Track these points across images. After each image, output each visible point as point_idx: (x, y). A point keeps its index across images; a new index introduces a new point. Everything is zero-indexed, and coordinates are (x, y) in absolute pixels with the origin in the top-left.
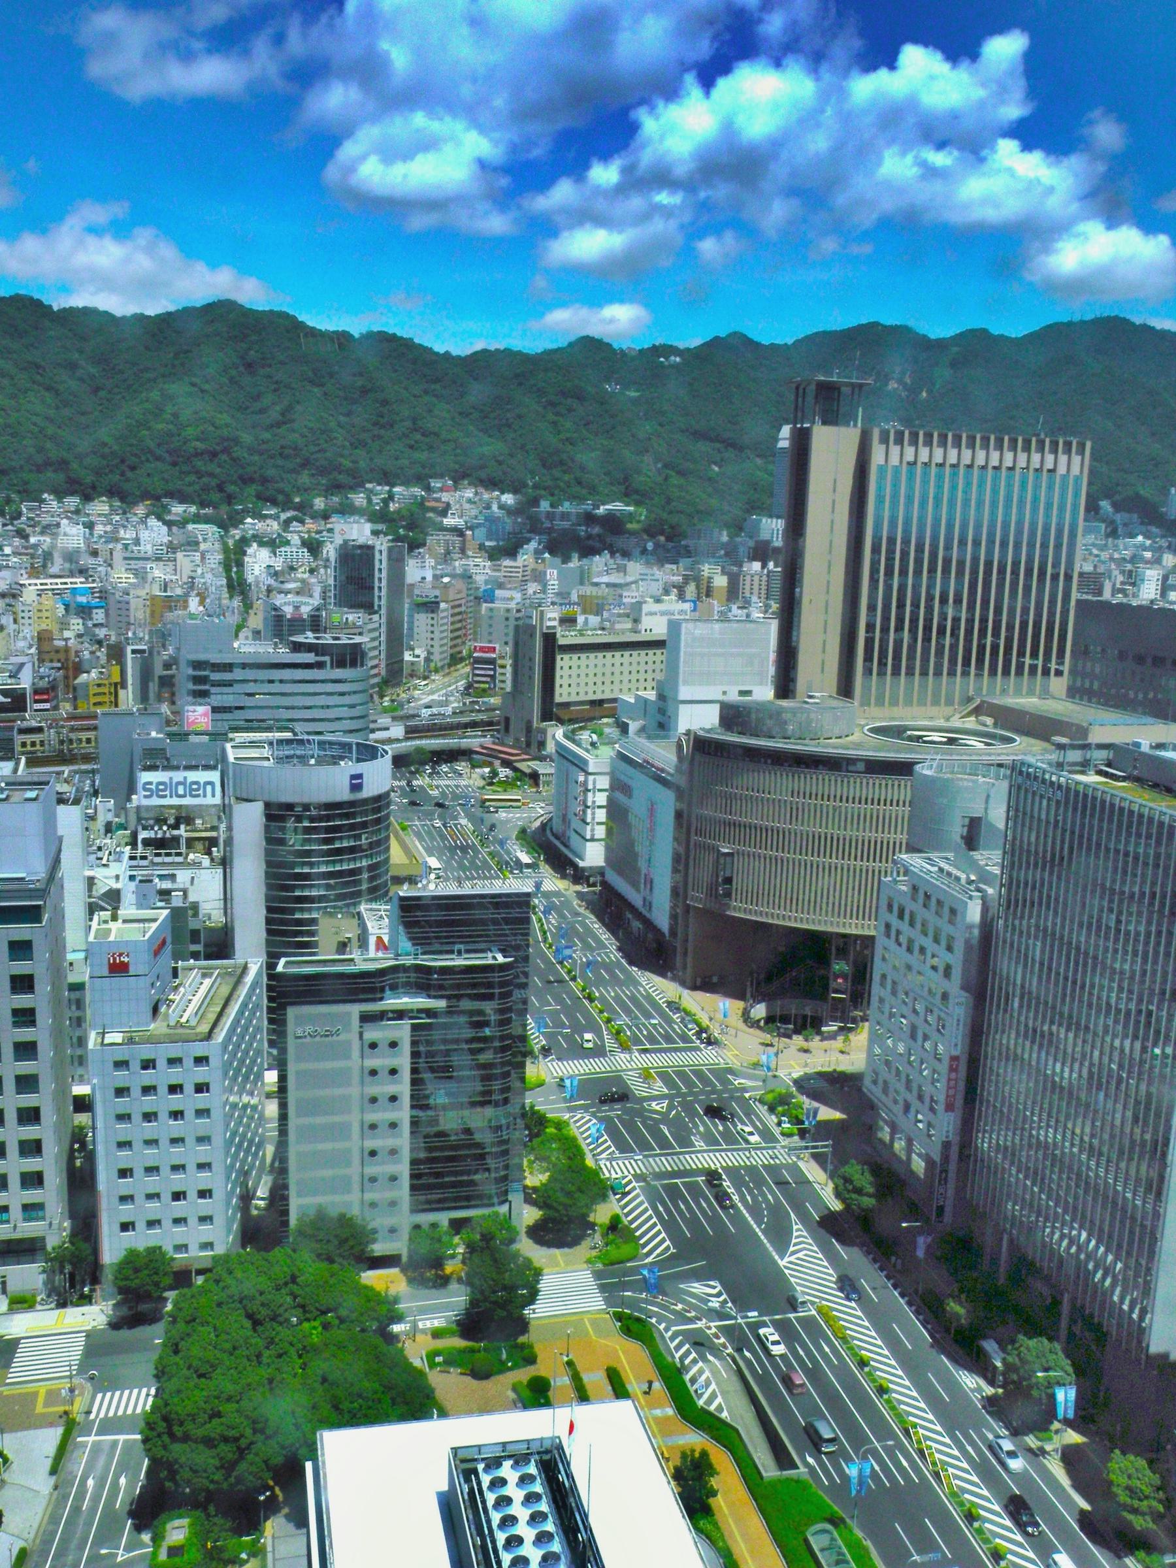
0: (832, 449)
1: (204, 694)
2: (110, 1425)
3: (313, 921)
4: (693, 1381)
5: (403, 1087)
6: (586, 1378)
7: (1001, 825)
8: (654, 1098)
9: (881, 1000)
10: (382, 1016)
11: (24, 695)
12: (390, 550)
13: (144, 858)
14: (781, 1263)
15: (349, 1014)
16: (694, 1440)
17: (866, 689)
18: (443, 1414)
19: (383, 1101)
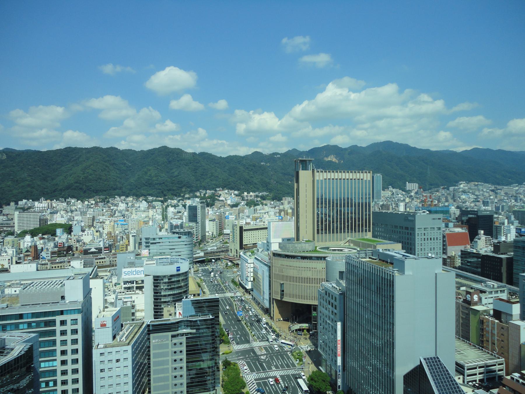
0: (305, 176)
1: (149, 246)
5: (184, 356)
10: (178, 335)
12: (201, 206)
15: (168, 335)
19: (178, 361)
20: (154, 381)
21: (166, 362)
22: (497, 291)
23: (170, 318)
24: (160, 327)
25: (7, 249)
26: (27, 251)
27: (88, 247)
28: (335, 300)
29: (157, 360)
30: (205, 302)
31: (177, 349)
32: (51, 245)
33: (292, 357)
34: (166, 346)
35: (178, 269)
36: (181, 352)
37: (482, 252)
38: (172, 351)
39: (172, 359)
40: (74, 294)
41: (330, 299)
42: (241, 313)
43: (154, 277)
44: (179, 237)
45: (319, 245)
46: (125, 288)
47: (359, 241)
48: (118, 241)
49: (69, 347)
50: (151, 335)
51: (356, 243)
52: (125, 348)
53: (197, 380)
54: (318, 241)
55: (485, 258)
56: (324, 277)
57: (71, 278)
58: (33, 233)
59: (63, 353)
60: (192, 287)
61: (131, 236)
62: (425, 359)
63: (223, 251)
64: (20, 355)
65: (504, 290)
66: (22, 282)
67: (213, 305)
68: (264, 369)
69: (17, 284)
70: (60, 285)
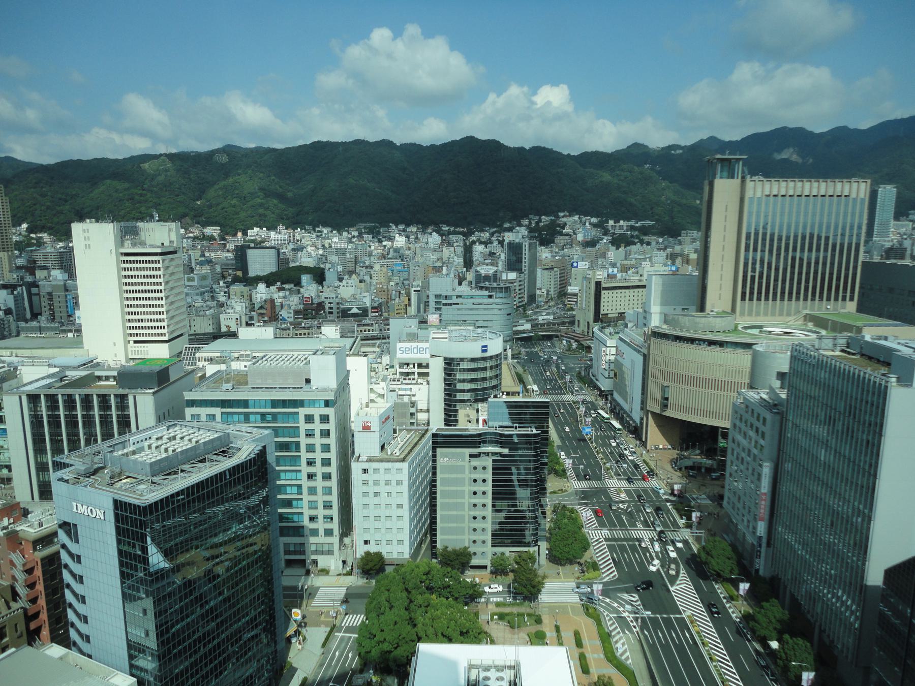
0: (725, 189)
2: (349, 630)
4: (617, 642)
5: (489, 488)
6: (554, 634)
8: (622, 502)
10: (478, 455)
12: (530, 245)
16: (610, 671)
17: (743, 308)
18: (493, 642)
23: (469, 426)
25: (234, 304)
26: (261, 308)
27: (347, 305)
29: (447, 488)
31: (479, 476)
32: (295, 299)
34: (461, 469)
35: (484, 349)
39: (470, 491)
40: (324, 376)
42: (589, 430)
44: (490, 297)
46: (402, 374)
48: (393, 297)
49: (318, 456)
51: (820, 322)
53: (508, 527)
54: (742, 314)
56: (747, 381)
58: (269, 280)
59: (310, 463)
60: (508, 381)
61: (412, 290)
63: (563, 324)
66: (254, 354)
67: (540, 412)
68: (622, 524)
69: (247, 356)
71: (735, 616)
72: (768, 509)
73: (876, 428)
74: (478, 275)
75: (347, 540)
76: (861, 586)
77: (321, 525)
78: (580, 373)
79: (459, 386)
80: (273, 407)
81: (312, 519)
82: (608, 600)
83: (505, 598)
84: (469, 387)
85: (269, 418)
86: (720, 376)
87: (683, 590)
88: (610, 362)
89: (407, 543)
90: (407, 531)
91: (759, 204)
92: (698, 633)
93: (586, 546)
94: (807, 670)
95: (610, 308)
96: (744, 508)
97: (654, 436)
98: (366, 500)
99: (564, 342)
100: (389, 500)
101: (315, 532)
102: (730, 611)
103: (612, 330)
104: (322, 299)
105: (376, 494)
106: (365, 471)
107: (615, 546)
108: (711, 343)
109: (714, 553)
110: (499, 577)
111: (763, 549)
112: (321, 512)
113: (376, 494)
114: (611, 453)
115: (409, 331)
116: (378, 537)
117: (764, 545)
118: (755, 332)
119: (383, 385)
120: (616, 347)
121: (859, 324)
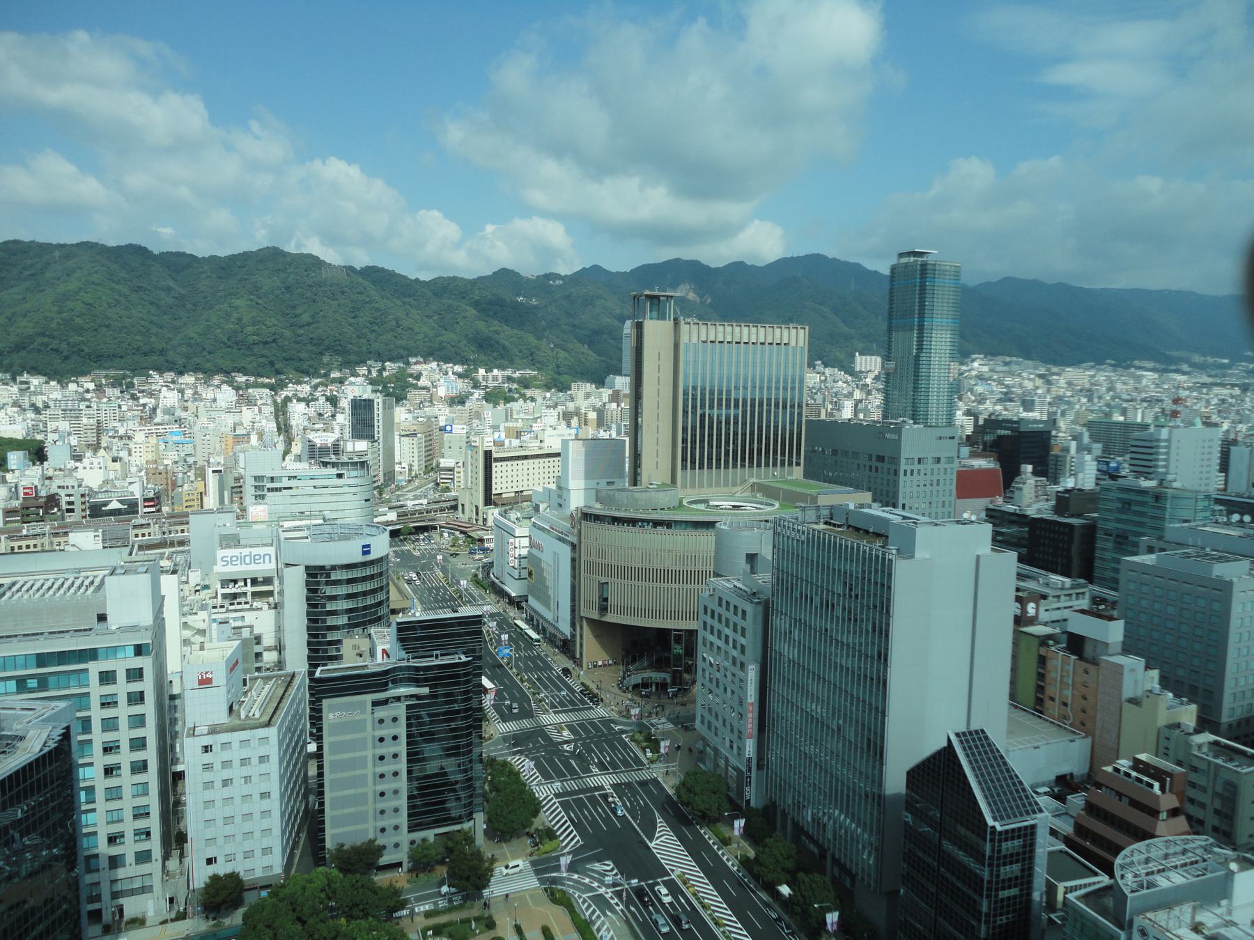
0: (656, 331)
3: (339, 642)
4: (599, 930)
5: (402, 748)
7: (770, 558)
8: (566, 742)
9: (704, 670)
10: (385, 702)
11: (136, 505)
12: (384, 402)
13: (222, 607)
14: (651, 845)
20: (331, 805)
21: (362, 762)
22: (1070, 595)
24: (346, 684)
27: (101, 498)
28: (744, 618)
30: (460, 624)
31: (386, 732)
33: (633, 745)
34: (360, 726)
35: (366, 550)
36: (395, 738)
37: (1032, 512)
38: (374, 737)
41: (730, 615)
42: (507, 651)
43: (307, 568)
44: (340, 476)
45: (687, 495)
46: (225, 596)
47: (778, 485)
48: (180, 483)
49: (124, 735)
50: (325, 703)
51: (770, 492)
52: (262, 732)
54: (684, 486)
55: (1036, 524)
57: (118, 571)
62: (957, 735)
63: (442, 510)
64: (46, 750)
65: (1083, 593)
68: (573, 772)
70: (91, 589)
71: (732, 865)
72: (756, 722)
73: (884, 608)
74: (311, 446)
75: (173, 864)
76: (880, 796)
77: (128, 848)
78: (476, 575)
79: (330, 606)
80: (39, 665)
81: (112, 840)
82: (576, 876)
83: (436, 904)
84: (345, 607)
85: (33, 683)
86: (669, 564)
87: (665, 844)
88: (521, 557)
89: (277, 850)
90: (277, 832)
91: (696, 352)
92: (694, 894)
93: (535, 807)
94: (830, 910)
95: (504, 486)
96: (724, 725)
97: (591, 649)
98: (208, 795)
99: (446, 535)
100: (246, 789)
101: (115, 862)
102: (725, 859)
103: (519, 515)
104: (54, 490)
105: (226, 783)
106: (207, 749)
107: (570, 802)
108: (657, 524)
109: (697, 789)
110: (421, 875)
111: (753, 775)
112: (129, 826)
113: (226, 783)
114: (539, 679)
115: (225, 532)
116: (229, 849)
117: (754, 768)
118: (701, 507)
119: (203, 615)
120: (530, 537)
121: (813, 492)
